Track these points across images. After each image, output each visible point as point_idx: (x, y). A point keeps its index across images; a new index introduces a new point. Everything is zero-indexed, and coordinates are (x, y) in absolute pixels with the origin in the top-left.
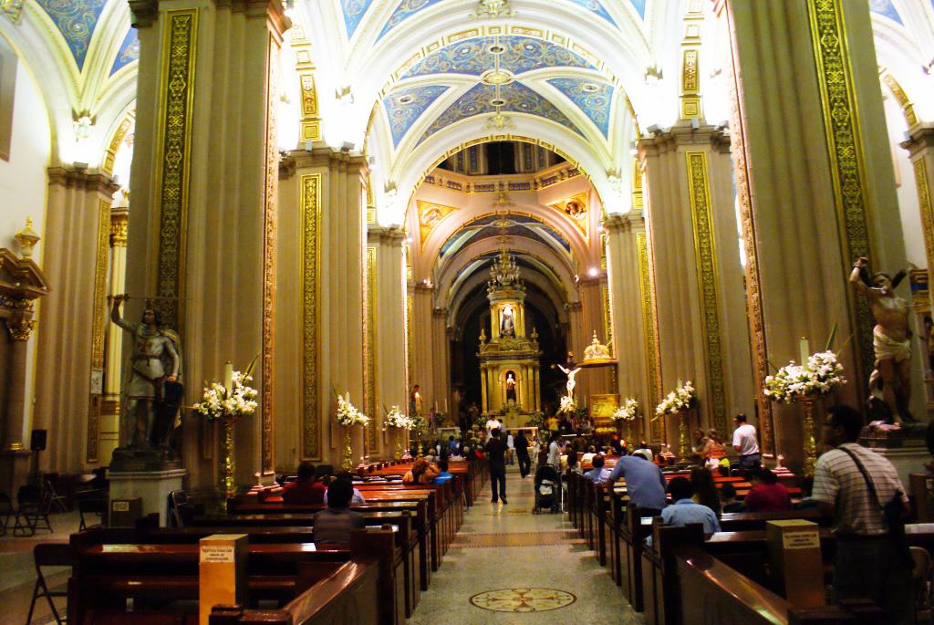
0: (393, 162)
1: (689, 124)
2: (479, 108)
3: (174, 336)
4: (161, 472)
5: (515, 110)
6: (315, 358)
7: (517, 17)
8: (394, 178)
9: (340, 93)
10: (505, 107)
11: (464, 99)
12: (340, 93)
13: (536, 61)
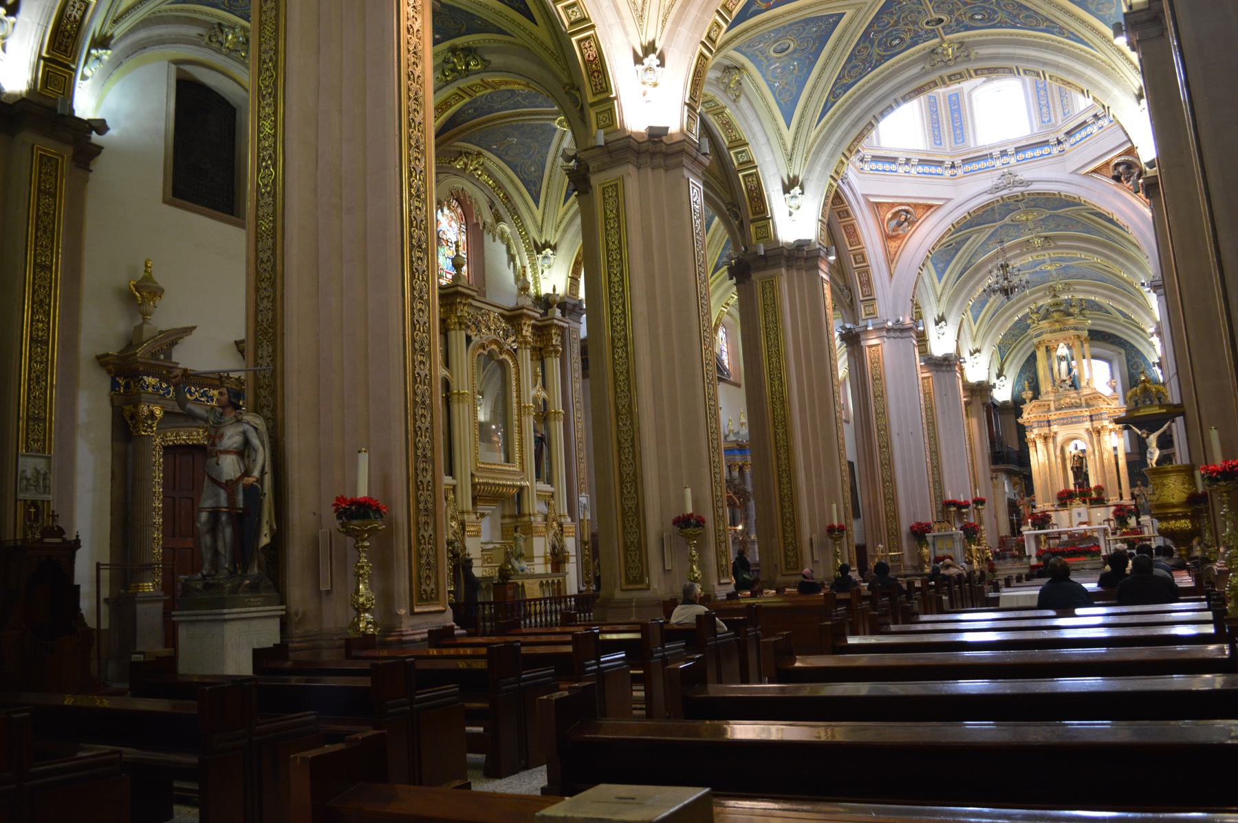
0: (789, 146)
2: (907, 37)
3: (259, 422)
4: (225, 611)
5: (968, 28)
6: (633, 440)
8: (798, 170)
9: (641, 54)
12: (641, 54)
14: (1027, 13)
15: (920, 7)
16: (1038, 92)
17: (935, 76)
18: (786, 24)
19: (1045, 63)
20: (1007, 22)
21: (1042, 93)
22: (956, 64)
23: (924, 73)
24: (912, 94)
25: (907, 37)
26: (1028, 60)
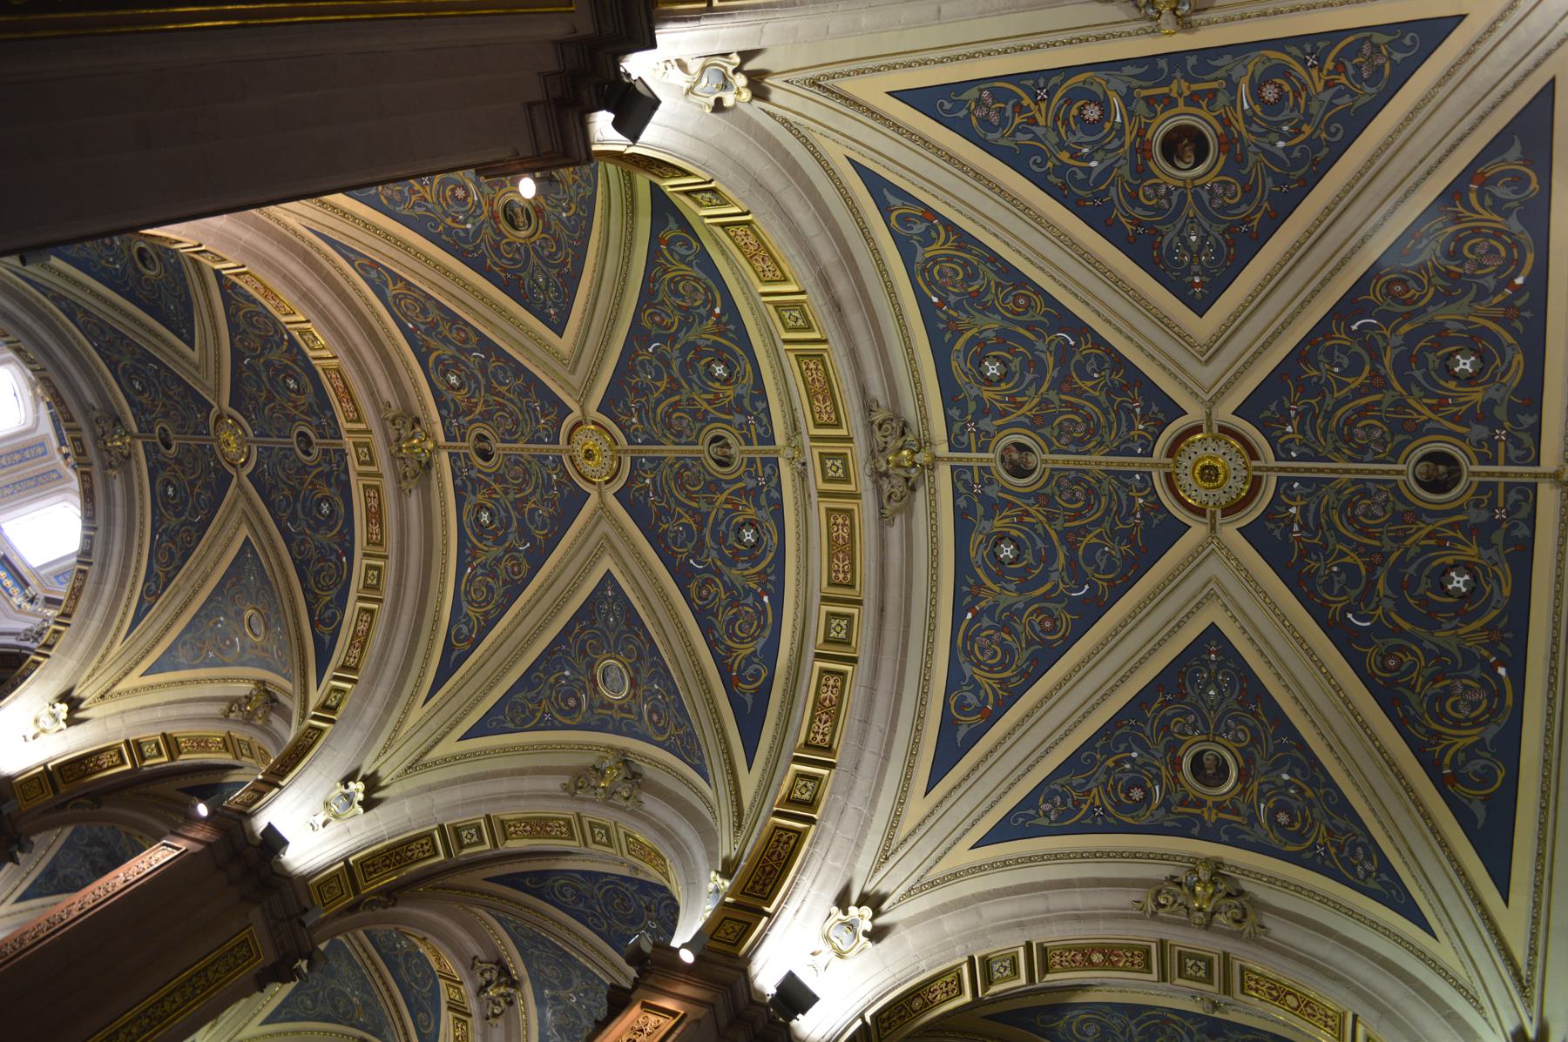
1: (306, 903)
7: (401, 494)
10: (157, 452)
11: (163, 373)
13: (293, 518)
14: (178, 555)
15: (191, 431)
16: (18, 452)
17: (80, 421)
18: (189, 281)
19: (103, 566)
20: (162, 523)
21: (17, 457)
22: (99, 452)
23: (86, 409)
24: (52, 390)
25: (145, 398)
26: (107, 544)
